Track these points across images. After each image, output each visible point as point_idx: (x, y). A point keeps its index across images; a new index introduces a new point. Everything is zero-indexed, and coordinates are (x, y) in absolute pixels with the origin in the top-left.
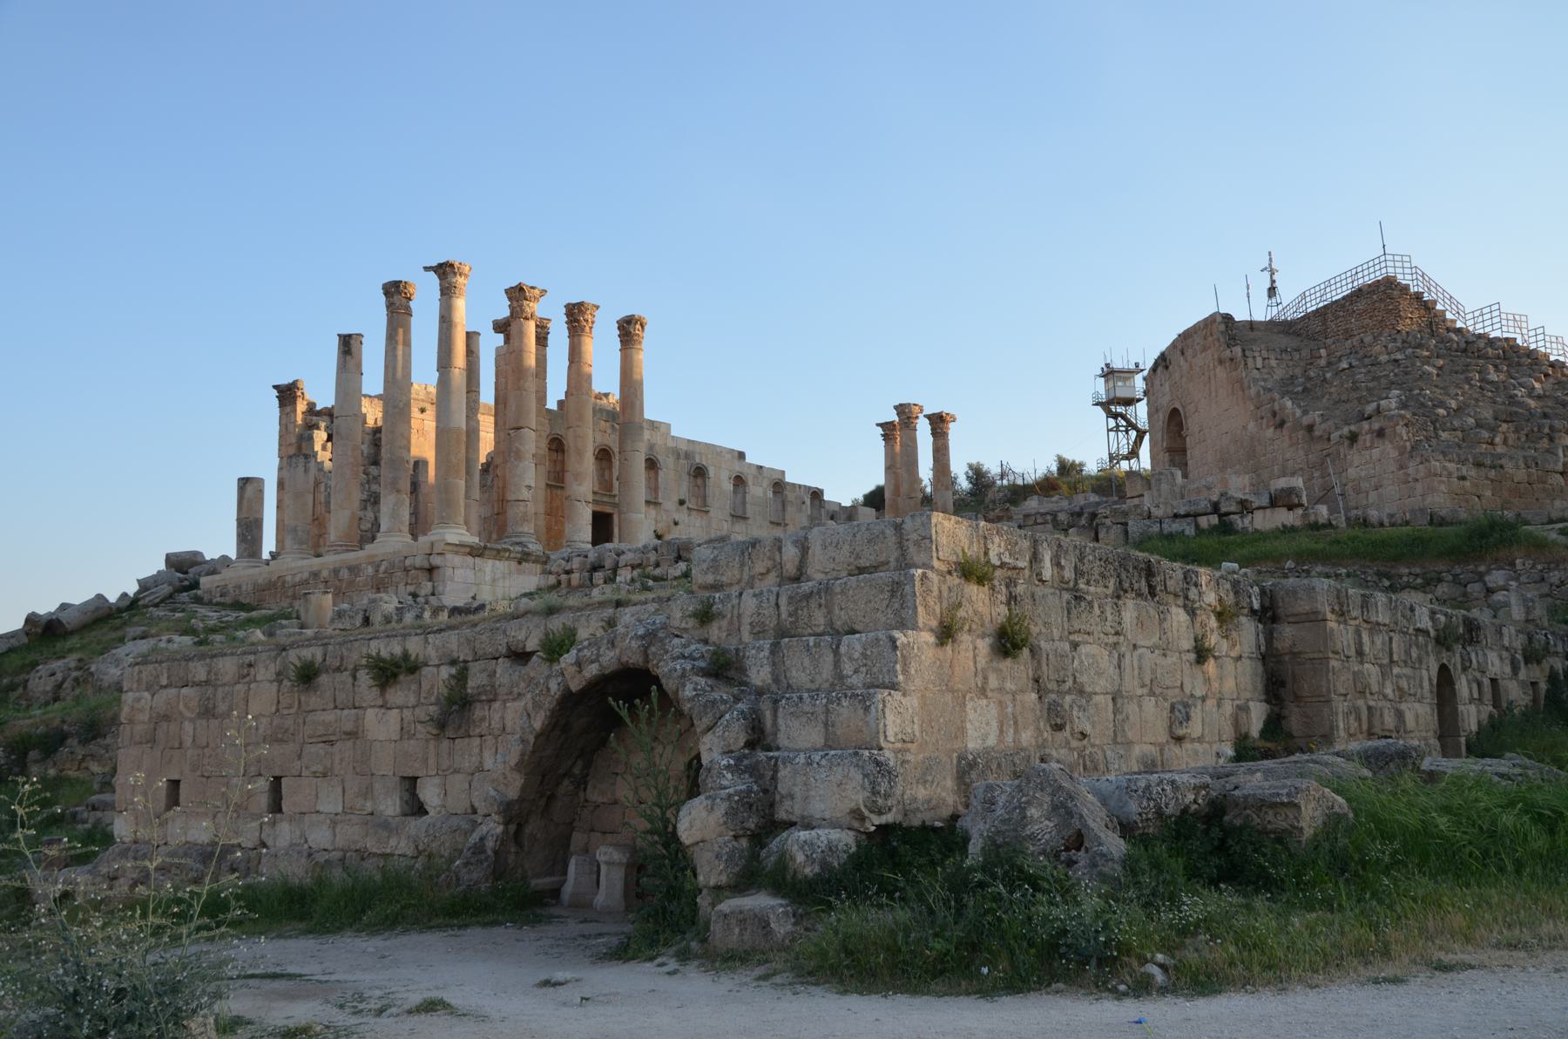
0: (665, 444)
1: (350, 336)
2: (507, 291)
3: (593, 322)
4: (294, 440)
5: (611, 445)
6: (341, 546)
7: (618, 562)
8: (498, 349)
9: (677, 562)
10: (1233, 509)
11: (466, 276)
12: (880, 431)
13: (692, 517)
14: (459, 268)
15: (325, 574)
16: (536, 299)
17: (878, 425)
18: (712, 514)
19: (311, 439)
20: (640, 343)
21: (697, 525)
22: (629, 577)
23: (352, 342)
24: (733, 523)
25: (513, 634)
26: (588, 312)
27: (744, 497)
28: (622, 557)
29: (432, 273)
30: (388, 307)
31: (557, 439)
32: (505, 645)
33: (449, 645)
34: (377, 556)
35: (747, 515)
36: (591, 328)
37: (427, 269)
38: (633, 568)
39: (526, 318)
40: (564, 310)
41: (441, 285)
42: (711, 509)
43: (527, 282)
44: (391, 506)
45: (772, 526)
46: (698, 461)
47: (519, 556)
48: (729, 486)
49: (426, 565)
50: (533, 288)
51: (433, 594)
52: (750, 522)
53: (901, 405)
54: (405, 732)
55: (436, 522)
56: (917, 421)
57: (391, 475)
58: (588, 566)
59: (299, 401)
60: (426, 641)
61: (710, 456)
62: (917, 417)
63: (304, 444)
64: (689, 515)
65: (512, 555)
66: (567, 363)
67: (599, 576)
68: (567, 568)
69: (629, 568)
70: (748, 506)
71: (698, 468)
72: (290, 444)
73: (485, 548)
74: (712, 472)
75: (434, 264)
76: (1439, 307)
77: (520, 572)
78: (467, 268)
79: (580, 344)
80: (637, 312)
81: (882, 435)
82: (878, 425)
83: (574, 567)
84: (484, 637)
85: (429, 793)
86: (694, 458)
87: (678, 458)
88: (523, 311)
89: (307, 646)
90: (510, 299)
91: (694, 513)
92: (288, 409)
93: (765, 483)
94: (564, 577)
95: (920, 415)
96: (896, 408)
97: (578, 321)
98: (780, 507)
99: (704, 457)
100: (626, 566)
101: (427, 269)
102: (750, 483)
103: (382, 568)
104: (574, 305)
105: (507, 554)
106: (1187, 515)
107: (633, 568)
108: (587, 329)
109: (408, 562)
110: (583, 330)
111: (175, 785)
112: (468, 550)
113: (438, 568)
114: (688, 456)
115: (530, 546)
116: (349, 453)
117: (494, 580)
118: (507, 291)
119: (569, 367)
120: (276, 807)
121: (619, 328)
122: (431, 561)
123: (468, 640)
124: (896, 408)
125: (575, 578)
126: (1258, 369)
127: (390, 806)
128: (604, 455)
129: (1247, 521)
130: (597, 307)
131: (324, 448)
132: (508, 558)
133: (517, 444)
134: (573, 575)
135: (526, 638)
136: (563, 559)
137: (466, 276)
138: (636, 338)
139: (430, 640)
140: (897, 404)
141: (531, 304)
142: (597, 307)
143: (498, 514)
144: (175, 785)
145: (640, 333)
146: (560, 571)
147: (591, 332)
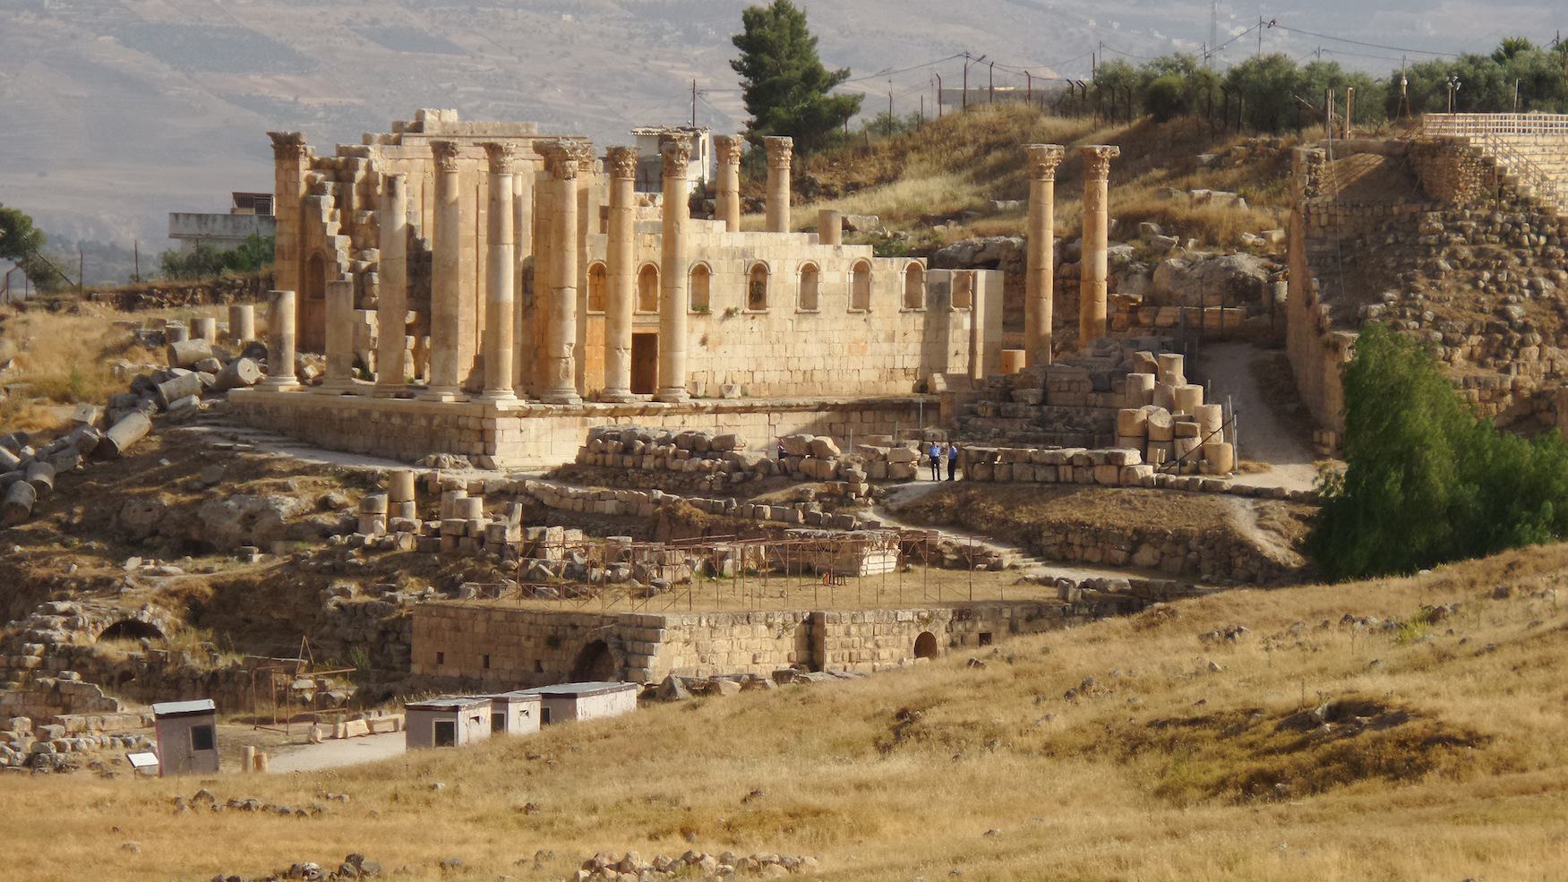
4: (296, 204)
10: (1081, 463)
15: (376, 415)
19: (317, 206)
24: (799, 322)
38: (656, 457)
39: (569, 178)
45: (851, 316)
46: (757, 256)
48: (795, 280)
49: (479, 428)
52: (821, 316)
54: (536, 645)
59: (302, 156)
63: (308, 210)
72: (292, 208)
74: (774, 267)
76: (1508, 174)
77: (562, 426)
79: (621, 188)
85: (545, 666)
87: (733, 258)
88: (565, 172)
92: (287, 164)
94: (599, 456)
97: (621, 167)
99: (765, 252)
102: (823, 269)
103: (436, 422)
106: (1050, 465)
109: (461, 422)
111: (441, 655)
114: (744, 254)
117: (538, 437)
120: (487, 665)
125: (609, 458)
126: (1322, 227)
127: (531, 668)
128: (647, 273)
129: (1090, 473)
131: (333, 218)
144: (441, 655)
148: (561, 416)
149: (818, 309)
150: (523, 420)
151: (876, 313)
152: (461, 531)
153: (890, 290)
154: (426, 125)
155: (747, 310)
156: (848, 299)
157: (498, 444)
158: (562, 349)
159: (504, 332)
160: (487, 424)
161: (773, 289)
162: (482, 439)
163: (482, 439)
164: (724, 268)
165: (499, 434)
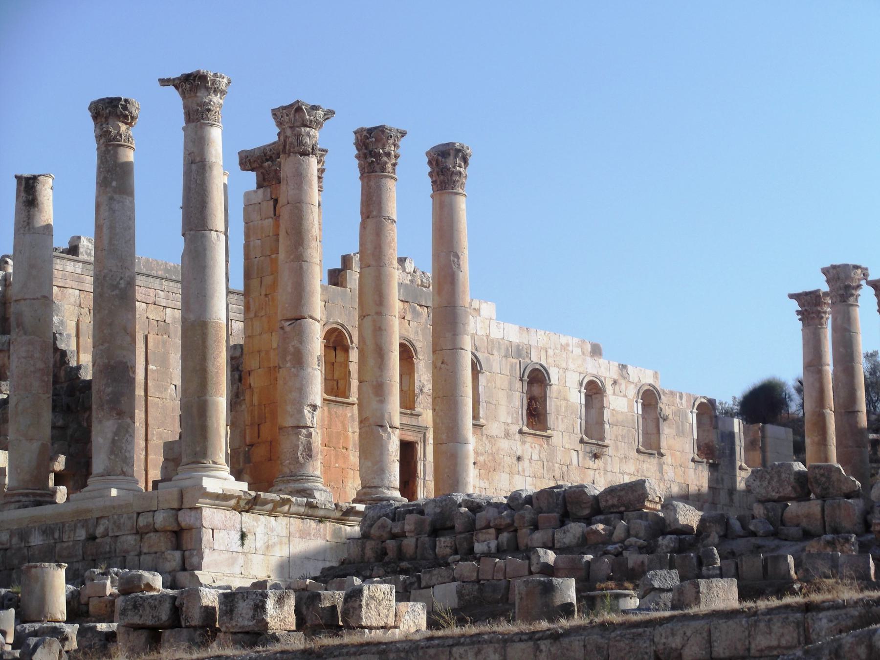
0: (488, 336)
1: (35, 178)
2: (275, 113)
3: (396, 157)
5: (412, 337)
6: (27, 495)
7: (474, 521)
8: (247, 195)
9: (562, 524)
11: (223, 93)
12: (795, 305)
13: (527, 445)
14: (214, 82)
16: (318, 124)
17: (792, 296)
18: (555, 440)
20: (463, 184)
21: (535, 457)
22: (493, 544)
23: (39, 187)
25: (663, 640)
26: (391, 141)
27: (601, 414)
28: (478, 515)
29: (172, 88)
30: (98, 137)
31: (336, 329)
32: (652, 654)
33: (572, 654)
34: (90, 511)
35: (607, 442)
36: (394, 165)
37: (164, 82)
38: (499, 531)
39: (305, 154)
40: (352, 138)
41: (185, 107)
42: (554, 433)
43: (308, 100)
44: (110, 435)
45: (641, 457)
46: (534, 359)
47: (302, 510)
48: (577, 398)
50: (315, 108)
51: (184, 569)
53: (834, 267)
55: (184, 460)
56: (860, 292)
57: (109, 390)
58: (428, 528)
60: (537, 649)
61: (550, 352)
62: (859, 286)
64: (524, 443)
65: (294, 509)
66: (359, 219)
67: (444, 543)
68: (396, 530)
69: (492, 531)
70: (607, 426)
71: (535, 371)
73: (256, 498)
74: (554, 375)
75: (176, 74)
78: (225, 81)
80: (458, 139)
81: (798, 313)
82: (792, 296)
83: (407, 528)
84: (622, 645)
86: (529, 354)
88: (300, 143)
89: (355, 654)
90: (280, 124)
91: (529, 439)
93: (632, 392)
94: (391, 544)
95: (863, 282)
96: (825, 271)
97: (378, 156)
98: (652, 428)
100: (488, 527)
101: (164, 82)
102: (609, 390)
104: (370, 131)
105: (286, 508)
107: (499, 531)
108: (389, 165)
109: (142, 521)
110: (383, 169)
112: (233, 502)
113: (190, 529)
115: (317, 494)
116: (37, 355)
118: (275, 113)
119: (363, 226)
121: (430, 163)
122: (180, 519)
123: (599, 648)
124: (825, 271)
130: (403, 134)
132: (287, 514)
133: (295, 342)
134: (406, 542)
135: (683, 646)
136: (387, 515)
137: (223, 93)
138: (456, 178)
139: (543, 647)
140: (827, 264)
141: (313, 132)
142: (403, 134)
143: (252, 445)
145: (462, 170)
146: (385, 535)
147: (394, 171)
148: (302, 516)
149: (607, 442)
150: (246, 517)
151: (668, 459)
152: (164, 614)
153: (680, 433)
154: (81, 250)
155: (525, 429)
156: (636, 437)
157: (207, 552)
158: (301, 412)
159: (211, 369)
160: (185, 519)
161: (552, 405)
162: (178, 546)
163: (178, 546)
164: (496, 367)
165: (206, 535)
